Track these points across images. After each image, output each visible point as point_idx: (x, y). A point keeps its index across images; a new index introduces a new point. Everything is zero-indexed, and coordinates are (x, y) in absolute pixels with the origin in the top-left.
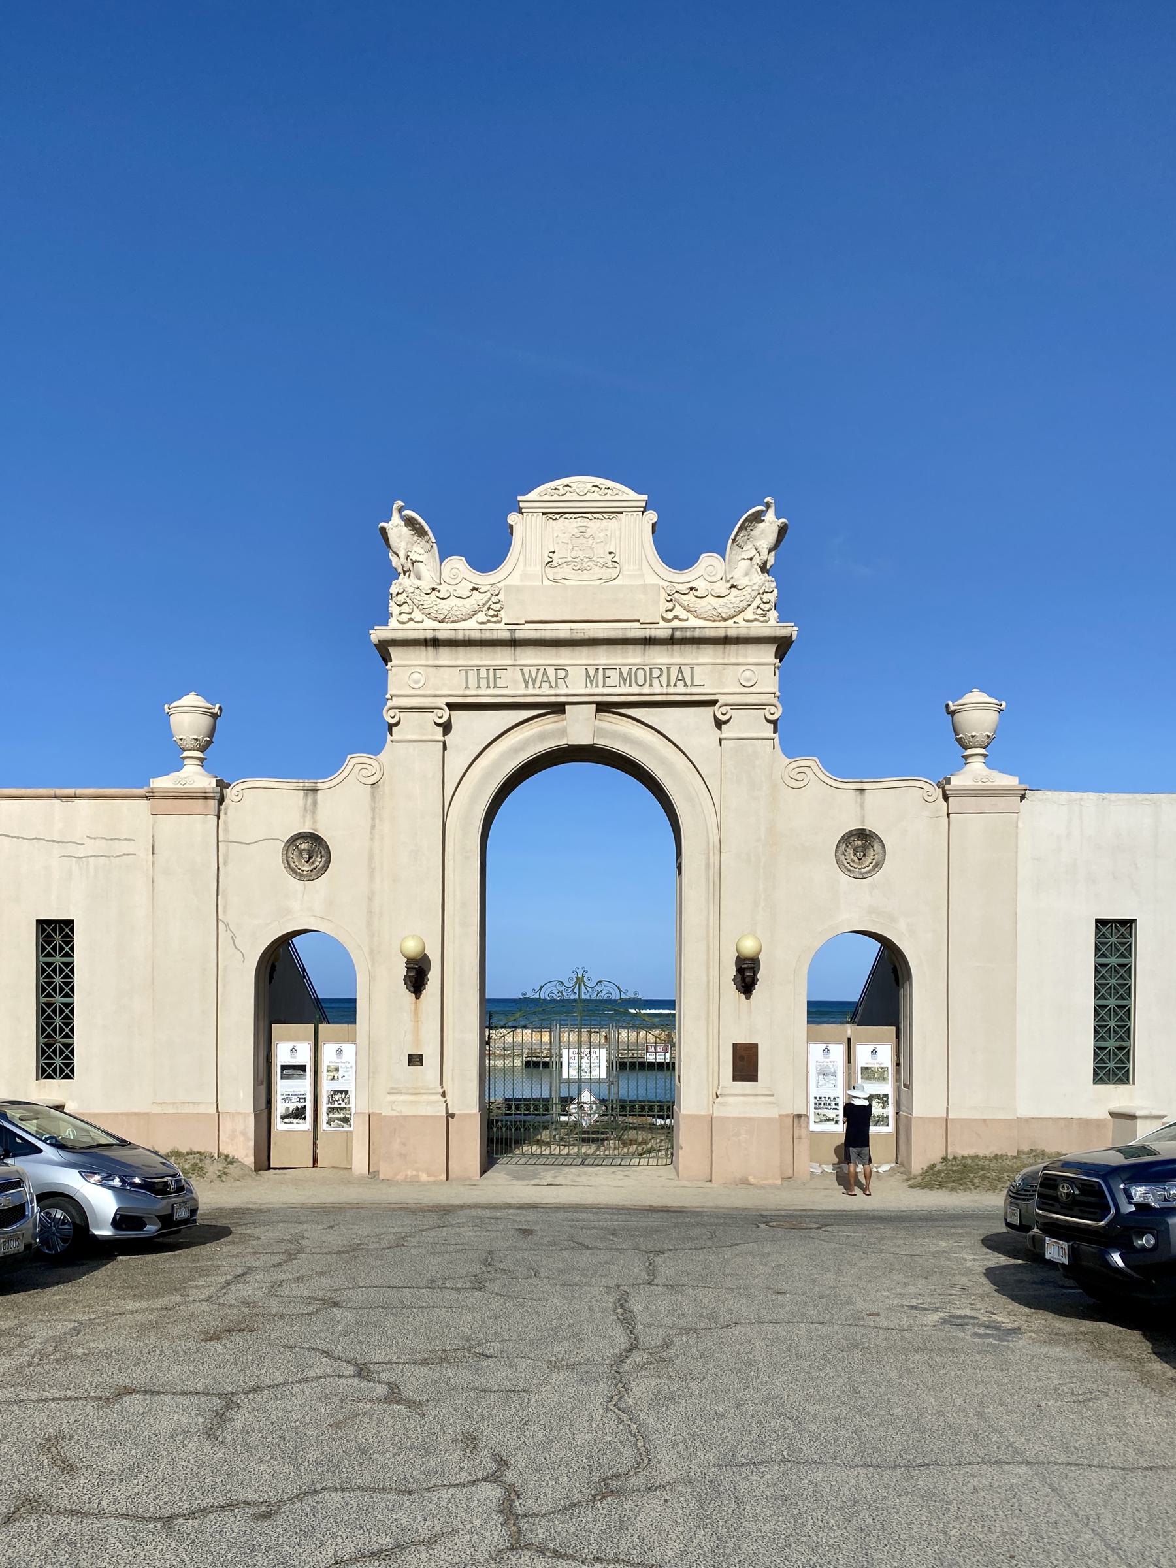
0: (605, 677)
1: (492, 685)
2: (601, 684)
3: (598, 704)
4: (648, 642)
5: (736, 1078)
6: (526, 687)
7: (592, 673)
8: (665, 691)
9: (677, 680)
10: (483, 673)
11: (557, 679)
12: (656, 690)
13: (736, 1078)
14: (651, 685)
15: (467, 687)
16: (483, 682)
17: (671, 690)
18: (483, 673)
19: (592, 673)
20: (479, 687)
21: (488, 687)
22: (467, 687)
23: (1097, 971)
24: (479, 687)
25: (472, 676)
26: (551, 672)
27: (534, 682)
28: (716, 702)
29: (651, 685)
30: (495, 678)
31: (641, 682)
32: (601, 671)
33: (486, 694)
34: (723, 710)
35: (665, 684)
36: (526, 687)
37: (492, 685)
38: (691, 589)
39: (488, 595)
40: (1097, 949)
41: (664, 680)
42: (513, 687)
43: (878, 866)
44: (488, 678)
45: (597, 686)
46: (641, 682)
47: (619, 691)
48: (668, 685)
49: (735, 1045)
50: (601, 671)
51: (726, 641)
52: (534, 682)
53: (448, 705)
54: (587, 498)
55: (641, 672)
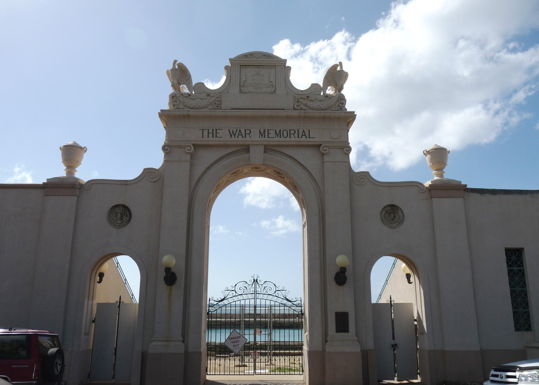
0: (268, 133)
1: (215, 136)
2: (266, 136)
3: (265, 145)
4: (289, 118)
5: (337, 331)
6: (231, 137)
7: (262, 132)
8: (297, 139)
9: (302, 135)
10: (211, 131)
11: (245, 134)
12: (293, 139)
13: (337, 331)
14: (290, 137)
15: (203, 137)
16: (211, 135)
17: (300, 139)
18: (211, 131)
19: (262, 132)
20: (208, 137)
21: (213, 137)
22: (203, 137)
23: (509, 274)
24: (208, 137)
25: (206, 132)
26: (243, 131)
27: (235, 135)
28: (321, 145)
29: (290, 137)
30: (216, 133)
31: (285, 136)
32: (266, 131)
33: (212, 140)
34: (325, 149)
35: (296, 136)
36: (231, 137)
37: (215, 136)
38: (308, 97)
39: (215, 98)
40: (507, 263)
41: (296, 135)
42: (224, 137)
43: (401, 222)
44: (213, 133)
45: (265, 137)
46: (285, 136)
47: (275, 140)
48: (298, 137)
49: (337, 314)
50: (266, 131)
51: (324, 119)
52: (235, 135)
53: (194, 145)
54: (261, 59)
55: (285, 132)
